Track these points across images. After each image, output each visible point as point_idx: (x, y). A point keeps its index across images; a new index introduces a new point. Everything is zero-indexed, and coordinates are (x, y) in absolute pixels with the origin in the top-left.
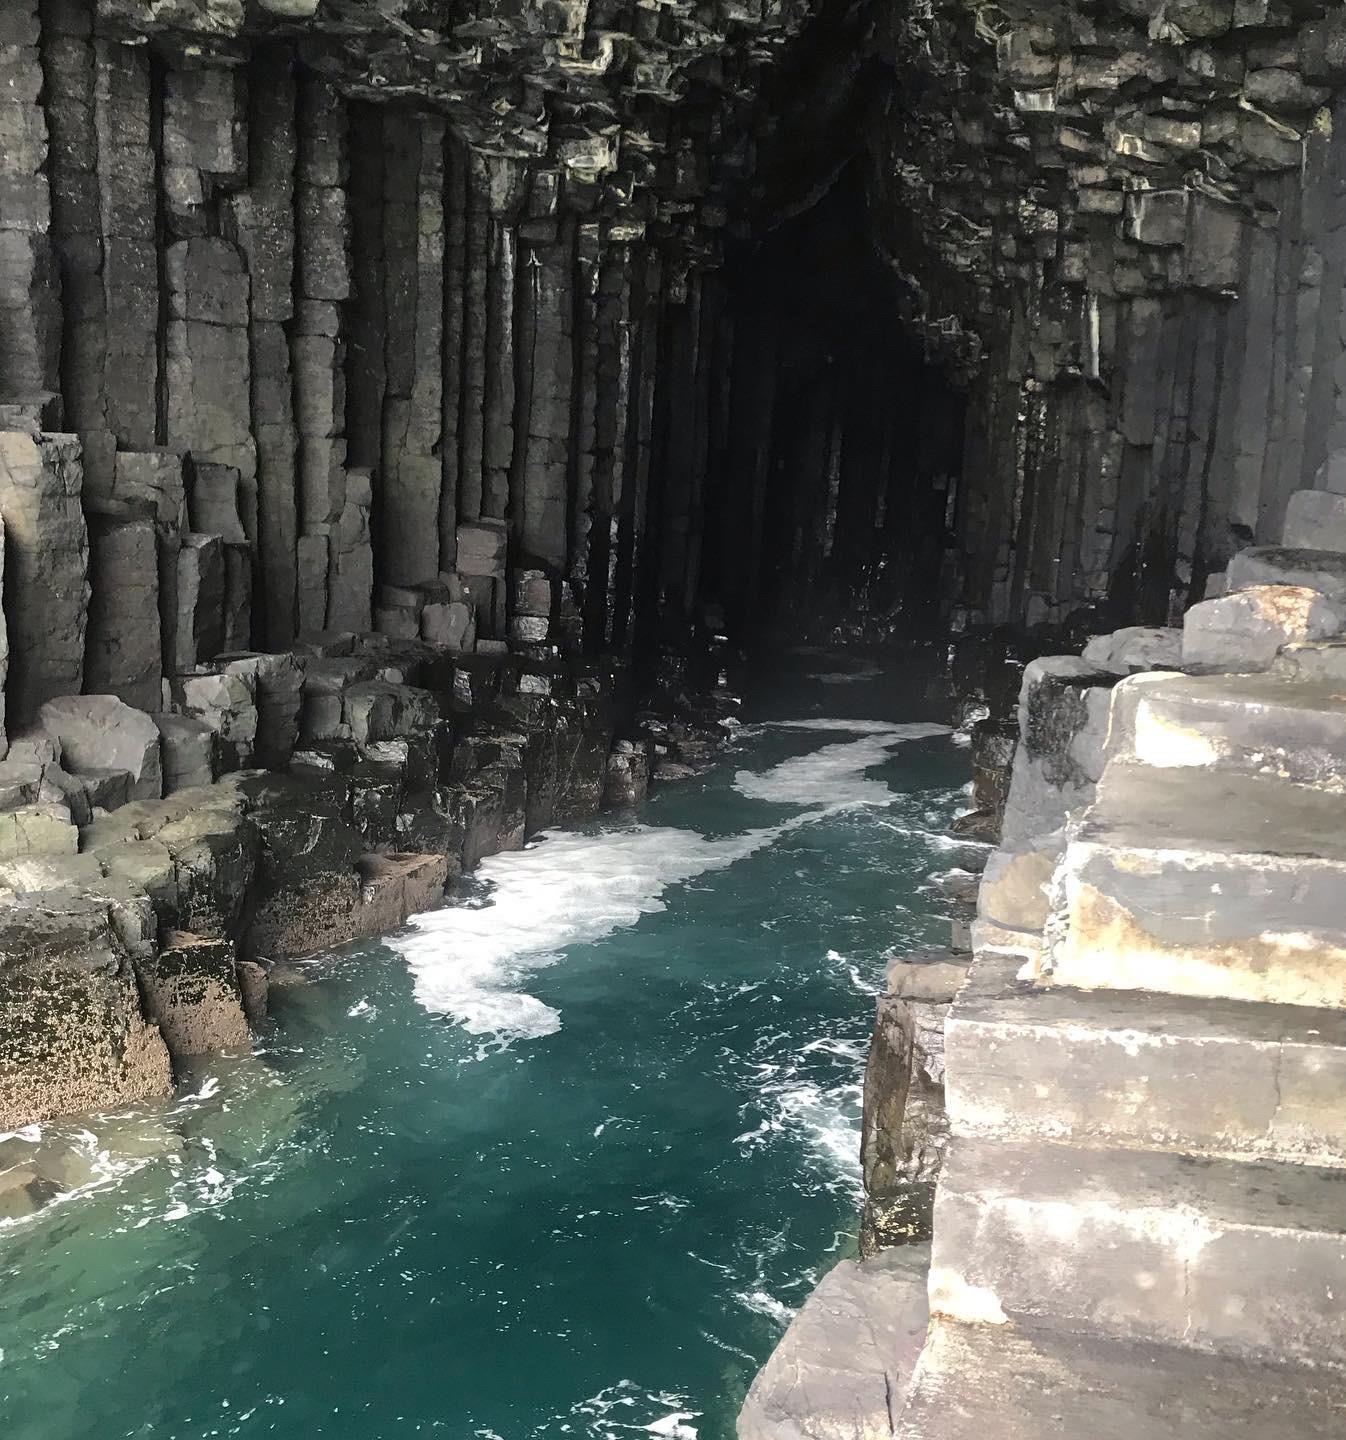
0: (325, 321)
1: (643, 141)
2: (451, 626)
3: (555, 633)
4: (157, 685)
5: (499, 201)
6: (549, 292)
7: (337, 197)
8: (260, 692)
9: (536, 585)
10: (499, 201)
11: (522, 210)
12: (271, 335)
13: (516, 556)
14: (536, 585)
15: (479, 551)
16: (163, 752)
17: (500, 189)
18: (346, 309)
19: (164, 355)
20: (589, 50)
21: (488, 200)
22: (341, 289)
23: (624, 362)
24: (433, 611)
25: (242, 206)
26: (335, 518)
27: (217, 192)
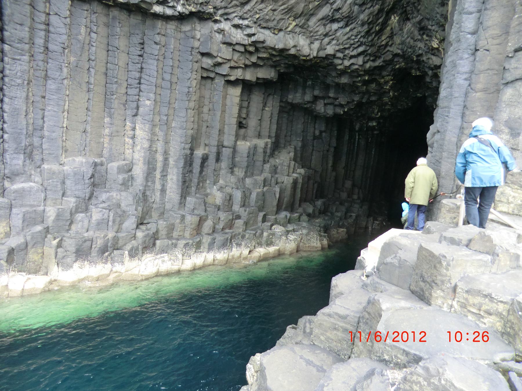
0: (332, 150)
1: (381, 121)
2: (344, 195)
3: (359, 198)
4: (312, 201)
5: (357, 129)
6: (363, 143)
7: (336, 132)
8: (324, 204)
9: (356, 190)
10: (357, 129)
11: (361, 130)
12: (325, 152)
13: (354, 185)
14: (356, 190)
15: (348, 184)
16: (314, 211)
17: (357, 127)
18: (335, 148)
19: (312, 155)
20: (377, 114)
21: (355, 129)
22: (335, 145)
23: (373, 153)
24: (342, 193)
25: (324, 134)
26: (330, 179)
27: (321, 132)
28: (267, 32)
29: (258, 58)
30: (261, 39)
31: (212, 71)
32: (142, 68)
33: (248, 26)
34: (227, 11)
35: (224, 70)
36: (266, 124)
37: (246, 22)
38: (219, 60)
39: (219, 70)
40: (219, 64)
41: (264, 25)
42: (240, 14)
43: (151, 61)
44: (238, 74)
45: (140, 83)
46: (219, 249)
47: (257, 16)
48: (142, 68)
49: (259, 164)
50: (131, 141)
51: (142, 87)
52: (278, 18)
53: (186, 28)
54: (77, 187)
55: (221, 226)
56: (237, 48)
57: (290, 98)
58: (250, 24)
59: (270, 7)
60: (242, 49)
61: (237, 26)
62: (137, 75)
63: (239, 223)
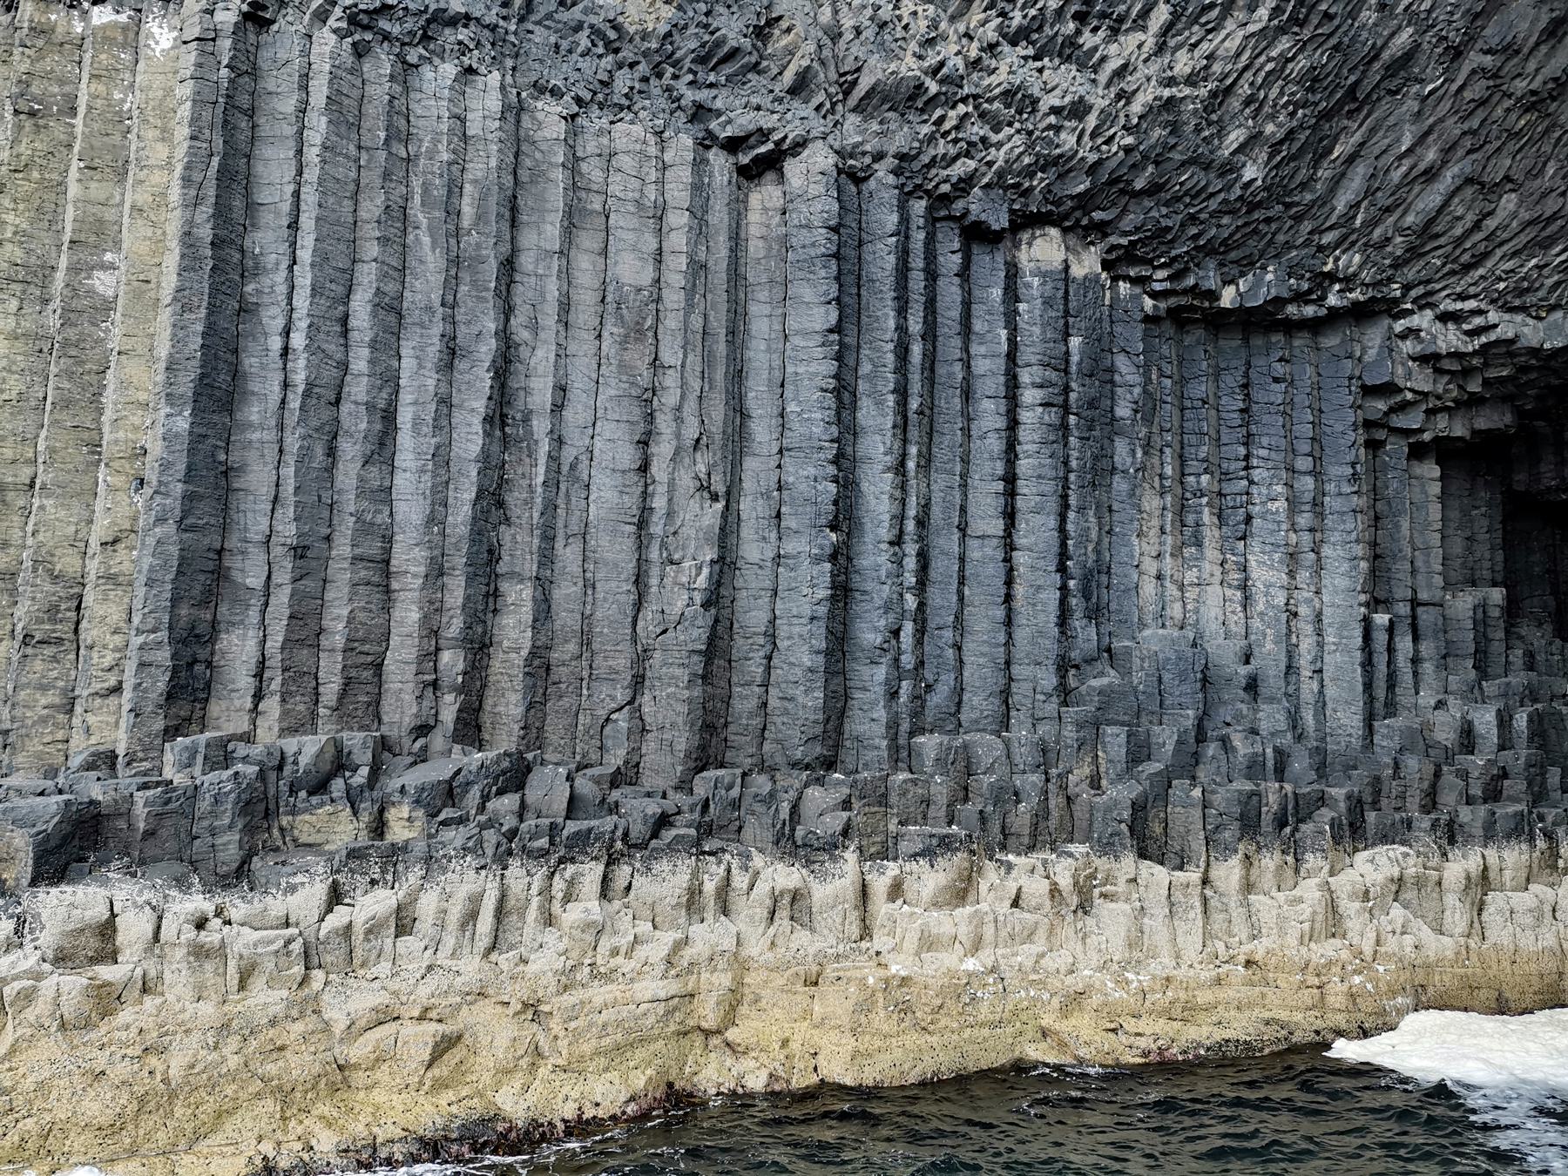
28: (1519, 318)
29: (1486, 383)
30: (1510, 335)
31: (1383, 426)
32: (1249, 435)
33: (1480, 312)
34: (1429, 287)
35: (1413, 420)
36: (1482, 550)
37: (1471, 304)
38: (1409, 396)
39: (1399, 421)
40: (1404, 407)
41: (1517, 303)
42: (1459, 290)
43: (1266, 419)
44: (1441, 425)
45: (1247, 468)
46: (1508, 837)
47: (1502, 286)
48: (1249, 435)
49: (1497, 647)
50: (1239, 593)
51: (1257, 474)
52: (1549, 282)
53: (1331, 341)
54: (1183, 688)
55: (1476, 791)
56: (1447, 364)
57: (1520, 479)
58: (1483, 306)
59: (1534, 262)
60: (1456, 367)
61: (1444, 318)
62: (1242, 451)
63: (1515, 786)
